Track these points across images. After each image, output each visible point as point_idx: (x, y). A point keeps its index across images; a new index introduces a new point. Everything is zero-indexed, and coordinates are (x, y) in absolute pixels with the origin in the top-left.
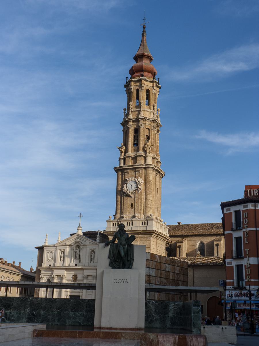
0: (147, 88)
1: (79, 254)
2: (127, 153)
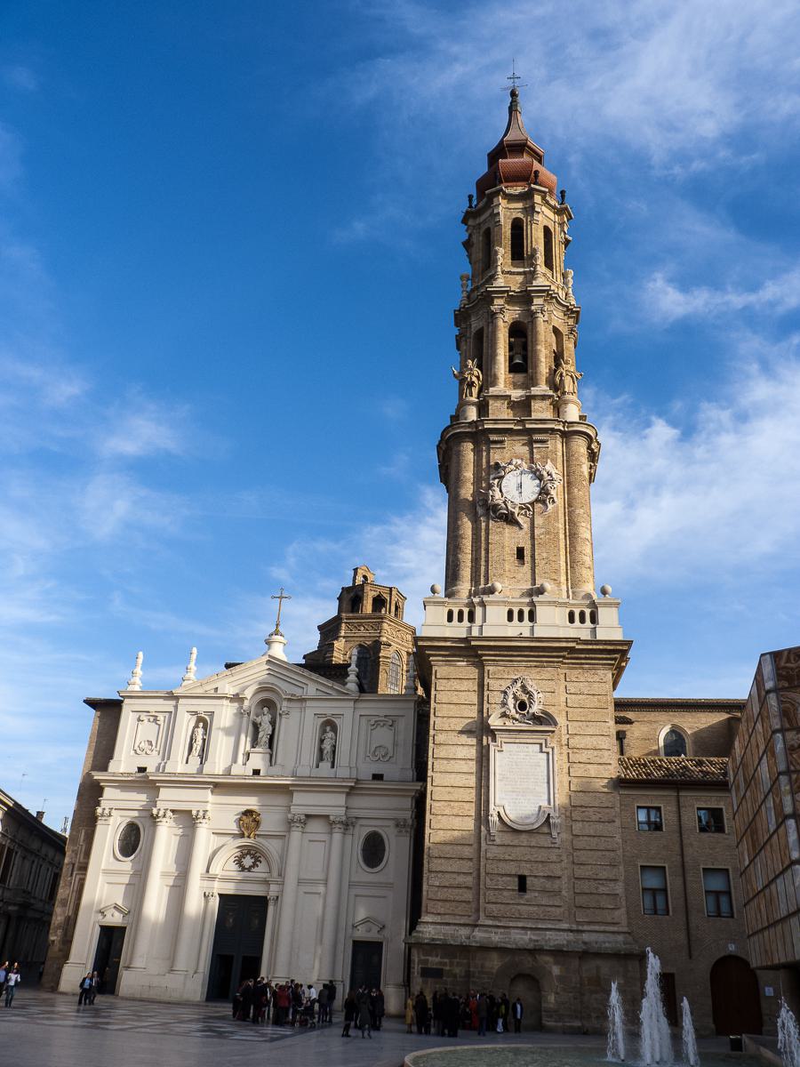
0: (546, 223)
1: (270, 733)
2: (493, 386)
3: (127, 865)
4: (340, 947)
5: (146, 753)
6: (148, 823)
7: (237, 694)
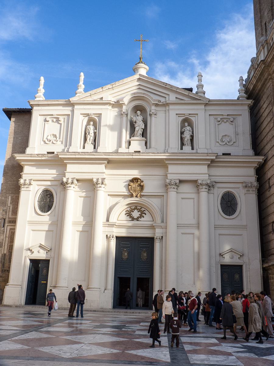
1: (143, 127)
3: (46, 218)
4: (214, 270)
5: (53, 143)
6: (59, 189)
7: (118, 102)
